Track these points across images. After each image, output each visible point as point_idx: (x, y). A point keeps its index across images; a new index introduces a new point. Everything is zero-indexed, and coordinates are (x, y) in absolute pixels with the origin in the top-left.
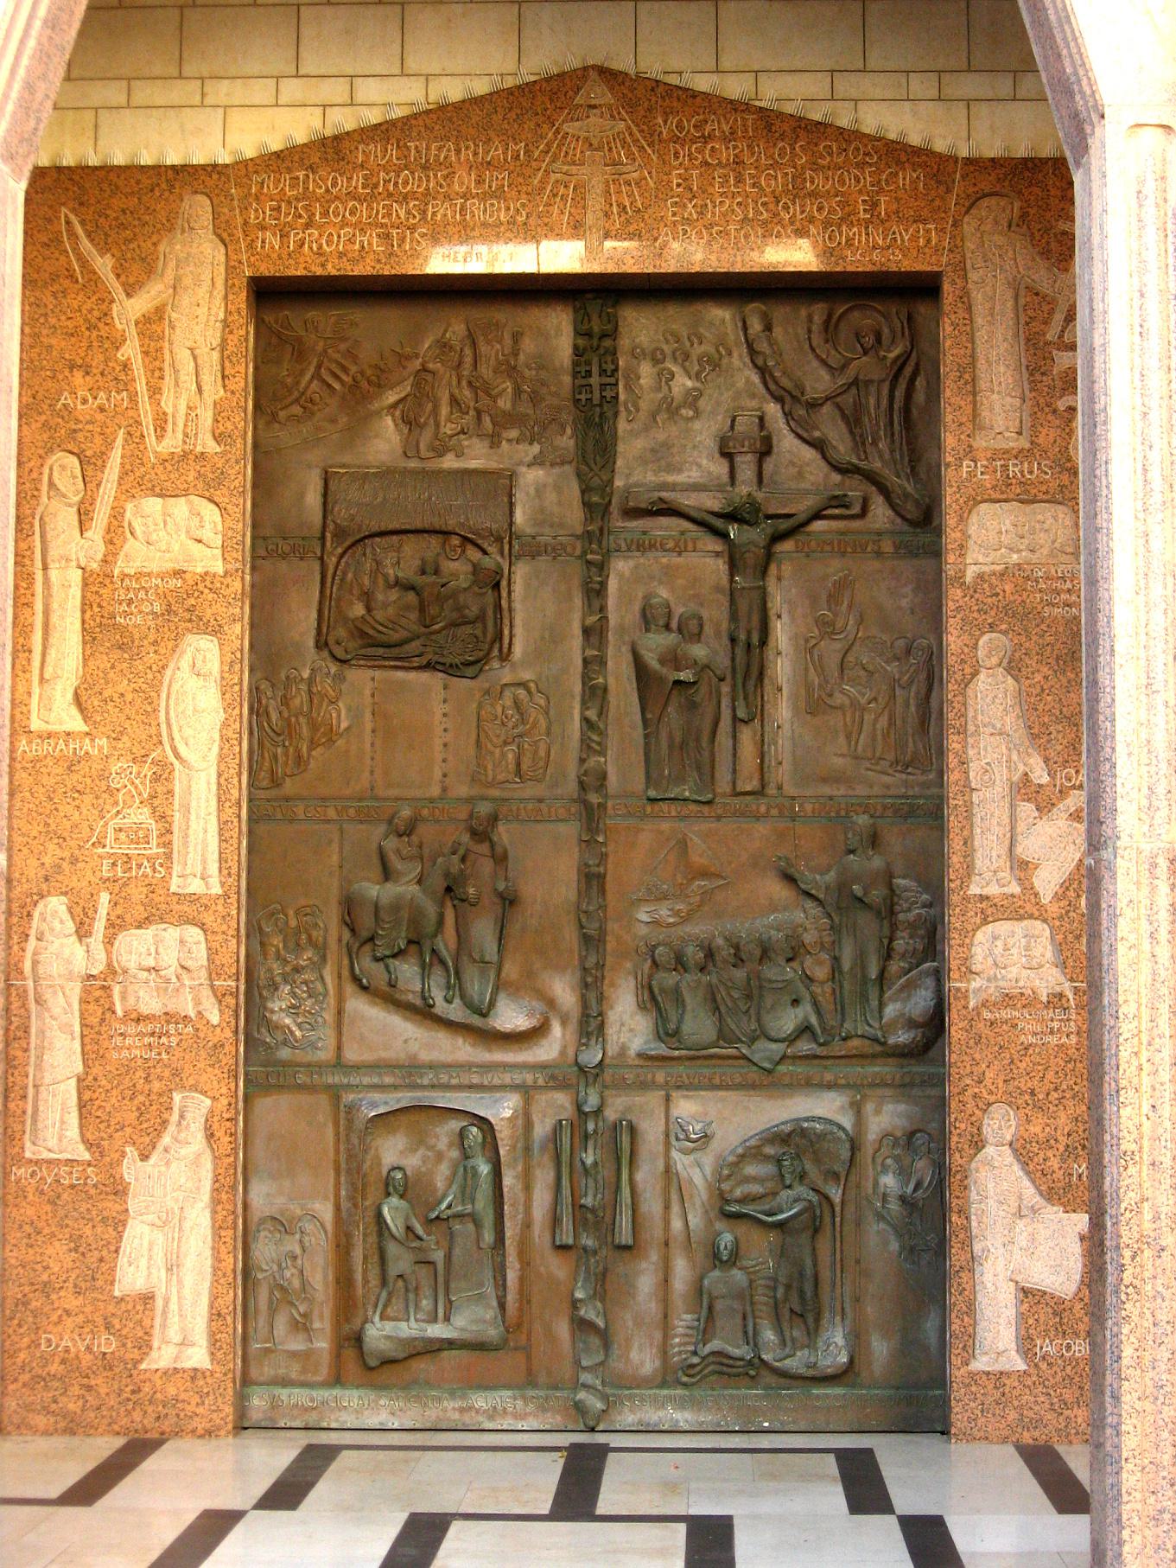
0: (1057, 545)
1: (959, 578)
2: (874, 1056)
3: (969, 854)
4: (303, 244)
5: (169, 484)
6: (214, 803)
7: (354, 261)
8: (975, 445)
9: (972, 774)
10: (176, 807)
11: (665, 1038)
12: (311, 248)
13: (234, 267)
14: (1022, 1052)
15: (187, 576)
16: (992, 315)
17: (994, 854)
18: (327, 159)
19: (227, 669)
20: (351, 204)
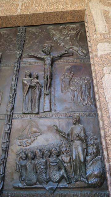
9: (107, 99)
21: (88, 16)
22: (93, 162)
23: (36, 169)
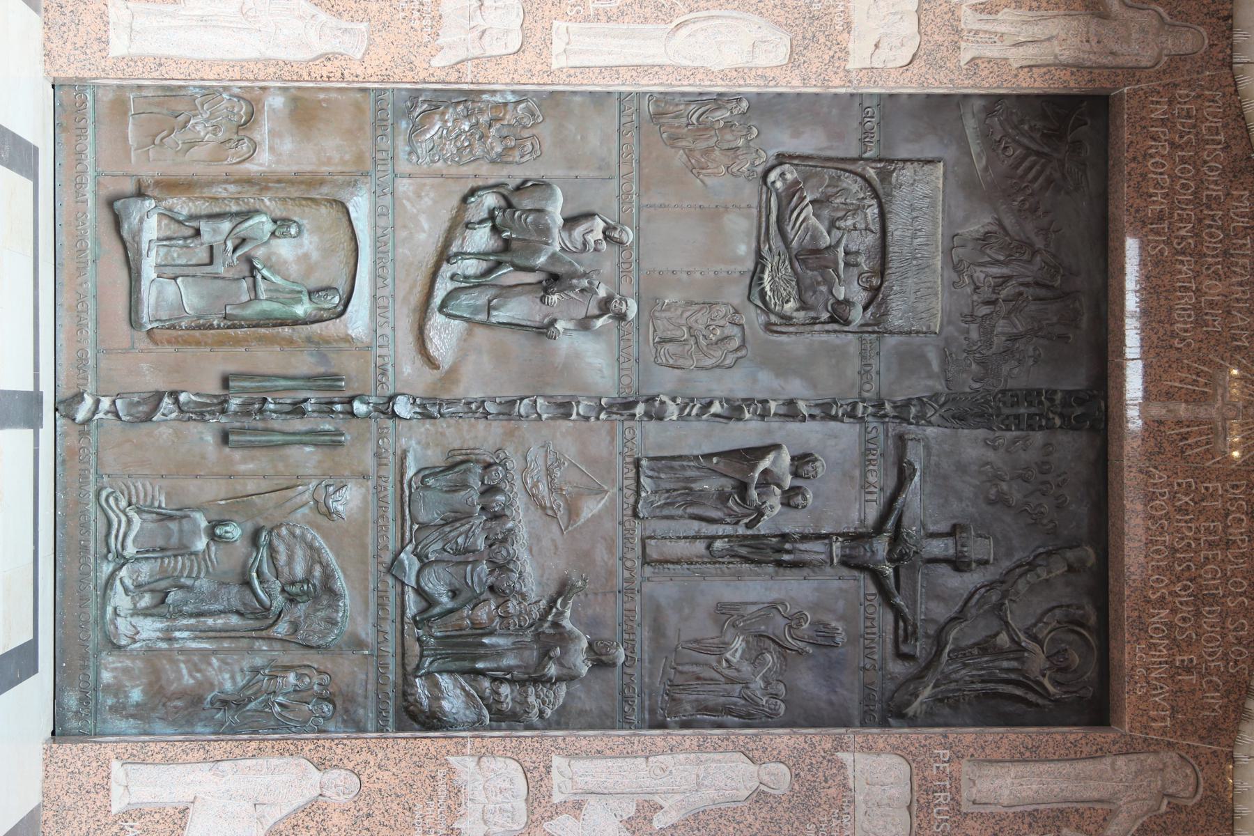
1: (840, 746)
2: (404, 666)
3: (588, 755)
4: (1155, 140)
5: (931, 16)
6: (637, 61)
7: (1138, 187)
8: (964, 761)
9: (661, 758)
10: (632, 26)
11: (420, 475)
12: (1151, 147)
13: (1134, 75)
14: (407, 806)
15: (845, 35)
16: (1085, 778)
17: (589, 779)
18: (1234, 161)
23: (456, 520)
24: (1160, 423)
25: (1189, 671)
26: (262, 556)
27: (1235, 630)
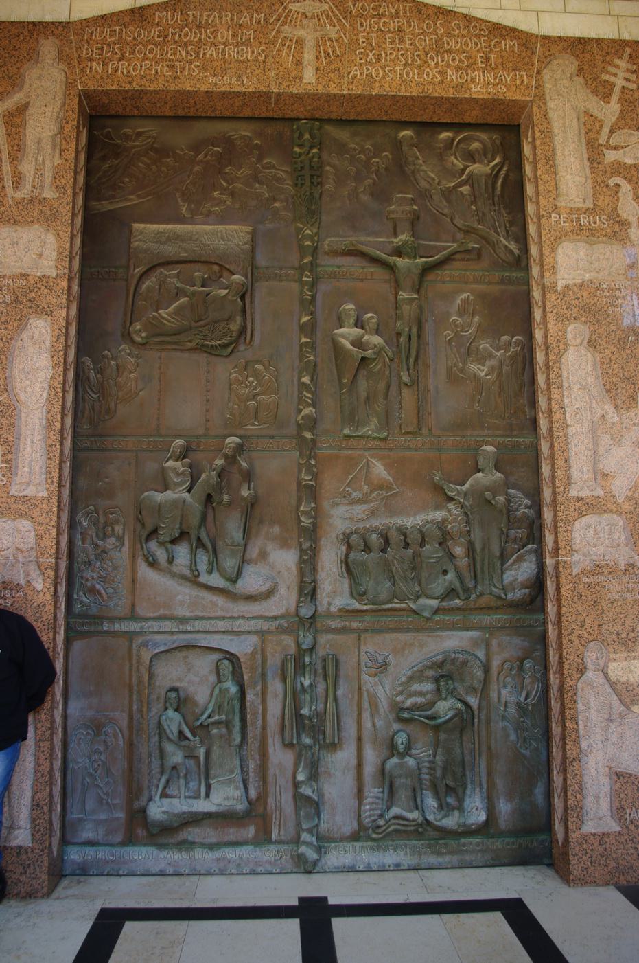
0: (613, 269)
1: (553, 287)
3: (568, 469)
4: (117, 70)
7: (150, 81)
8: (558, 204)
9: (568, 415)
12: (122, 72)
15: (30, 278)
19: (55, 340)
20: (149, 47)
21: (538, 134)
22: (517, 557)
24: (317, 69)
25: (488, 59)
26: (418, 716)
27: (459, 29)
